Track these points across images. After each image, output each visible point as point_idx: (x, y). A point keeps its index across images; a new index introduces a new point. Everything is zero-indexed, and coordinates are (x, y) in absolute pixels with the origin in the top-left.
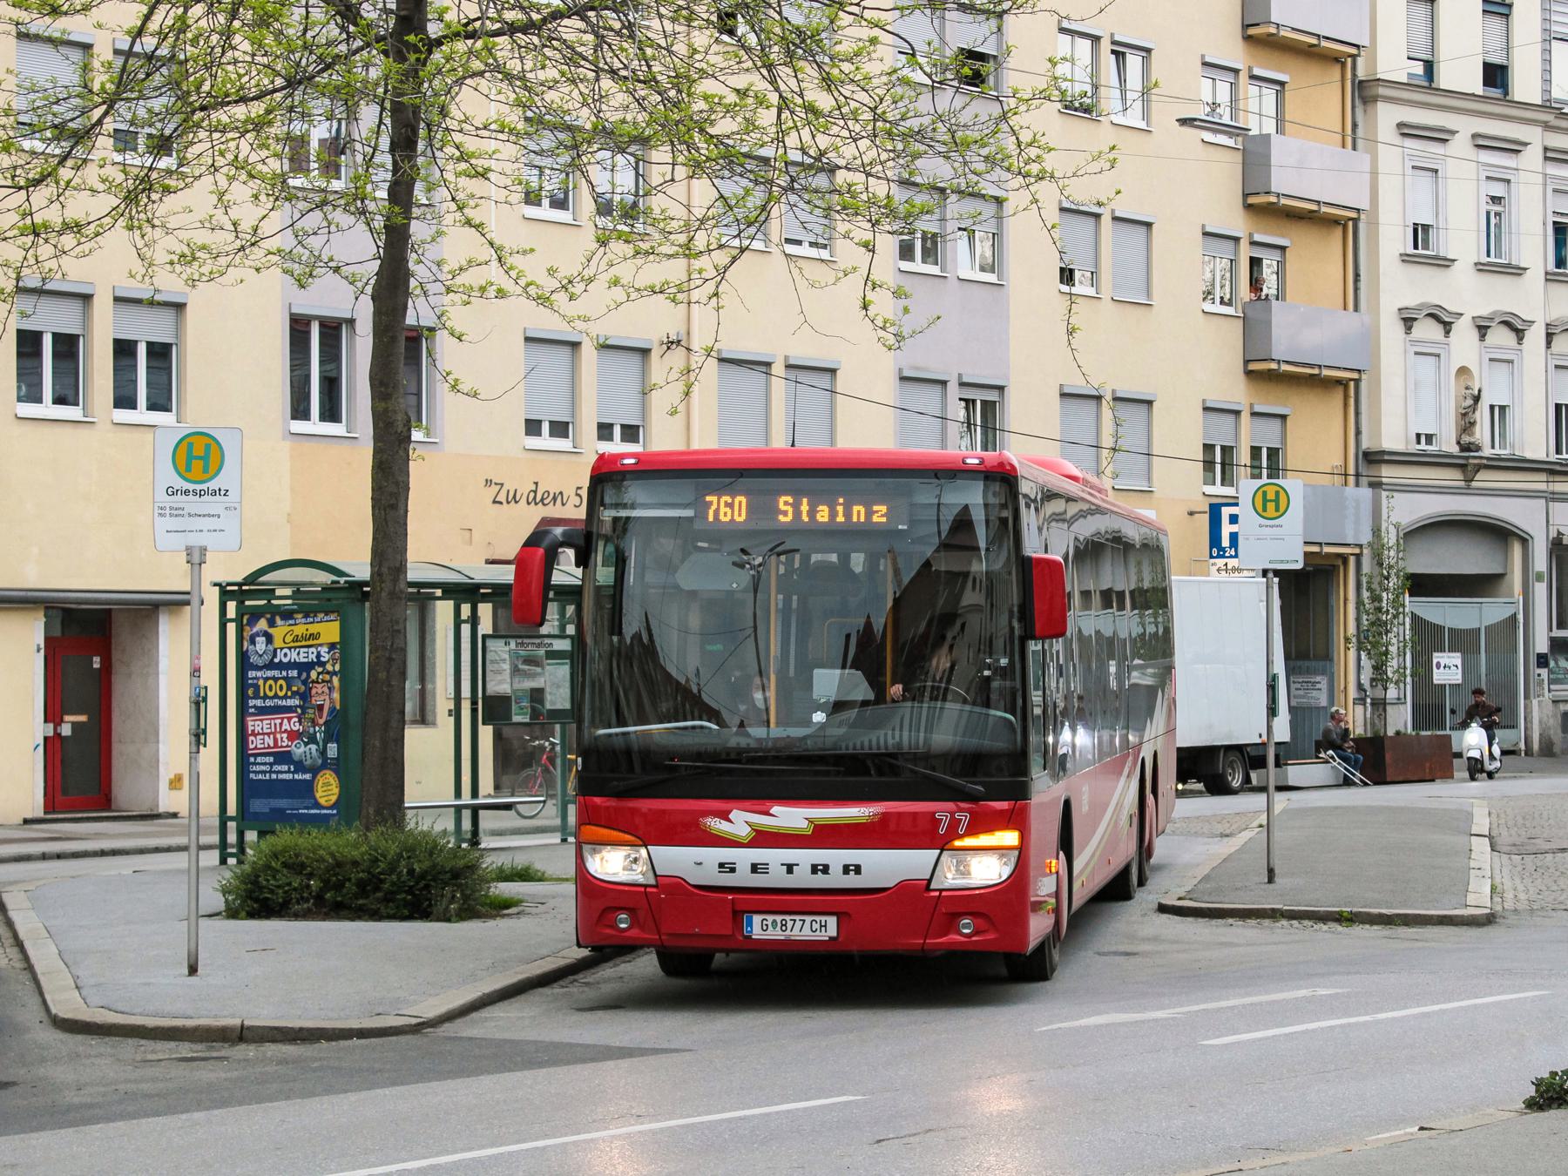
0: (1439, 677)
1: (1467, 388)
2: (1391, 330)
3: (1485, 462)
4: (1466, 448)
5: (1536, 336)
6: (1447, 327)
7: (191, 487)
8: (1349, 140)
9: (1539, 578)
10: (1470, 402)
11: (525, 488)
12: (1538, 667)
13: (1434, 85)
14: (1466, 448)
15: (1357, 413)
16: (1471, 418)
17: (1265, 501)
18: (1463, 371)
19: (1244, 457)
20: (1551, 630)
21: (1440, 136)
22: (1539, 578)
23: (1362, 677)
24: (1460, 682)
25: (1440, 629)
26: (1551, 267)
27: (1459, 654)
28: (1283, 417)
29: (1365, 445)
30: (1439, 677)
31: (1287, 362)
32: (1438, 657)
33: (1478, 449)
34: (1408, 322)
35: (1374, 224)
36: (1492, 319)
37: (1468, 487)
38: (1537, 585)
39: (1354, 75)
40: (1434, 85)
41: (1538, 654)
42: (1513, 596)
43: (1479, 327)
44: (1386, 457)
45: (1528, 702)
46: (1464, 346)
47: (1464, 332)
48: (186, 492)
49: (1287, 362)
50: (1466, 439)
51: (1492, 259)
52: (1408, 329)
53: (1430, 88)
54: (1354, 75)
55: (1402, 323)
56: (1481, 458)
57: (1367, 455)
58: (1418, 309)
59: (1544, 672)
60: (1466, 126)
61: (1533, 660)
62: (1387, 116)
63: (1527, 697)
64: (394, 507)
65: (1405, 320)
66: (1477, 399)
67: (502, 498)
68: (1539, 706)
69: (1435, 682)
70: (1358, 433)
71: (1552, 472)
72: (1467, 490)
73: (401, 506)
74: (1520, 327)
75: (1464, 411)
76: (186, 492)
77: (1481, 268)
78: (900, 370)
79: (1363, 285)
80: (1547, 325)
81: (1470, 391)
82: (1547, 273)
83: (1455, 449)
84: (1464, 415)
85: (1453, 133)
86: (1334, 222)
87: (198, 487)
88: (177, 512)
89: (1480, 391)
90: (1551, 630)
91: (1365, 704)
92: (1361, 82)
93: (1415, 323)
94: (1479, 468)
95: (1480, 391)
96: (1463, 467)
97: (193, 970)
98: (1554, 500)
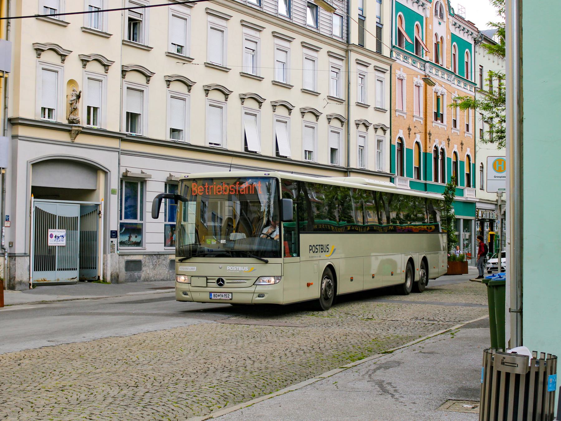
0: (51, 242)
1: (74, 91)
3: (81, 129)
4: (71, 122)
5: (115, 70)
6: (63, 57)
9: (113, 192)
10: (75, 98)
12: (111, 237)
14: (71, 122)
16: (74, 106)
20: (121, 219)
22: (113, 192)
23: (3, 241)
24: (65, 245)
25: (55, 216)
26: (126, 38)
27: (65, 230)
29: (10, 115)
30: (51, 242)
32: (50, 231)
33: (78, 122)
34: (39, 51)
38: (112, 196)
41: (111, 231)
42: (98, 200)
44: (20, 121)
45: (105, 255)
47: (73, 62)
50: (72, 117)
52: (39, 55)
55: (35, 52)
56: (79, 127)
57: (10, 120)
59: (115, 240)
61: (109, 234)
63: (105, 252)
66: (79, 97)
68: (111, 257)
69: (49, 244)
71: (123, 140)
72: (72, 144)
74: (106, 64)
75: (71, 102)
80: (123, 66)
81: (75, 92)
82: (123, 41)
83: (66, 122)
84: (71, 104)
89: (80, 92)
90: (121, 219)
91: (4, 256)
95: (80, 92)
96: (69, 131)
98: (122, 154)
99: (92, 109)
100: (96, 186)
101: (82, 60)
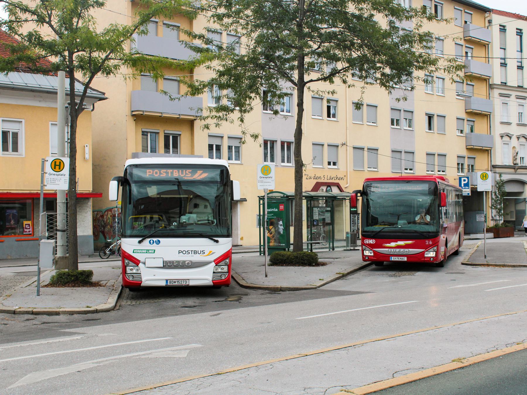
2: (498, 139)
6: (510, 137)
7: (265, 176)
8: (488, 97)
10: (516, 154)
11: (313, 176)
13: (507, 85)
14: (515, 164)
15: (491, 157)
17: (483, 176)
18: (514, 147)
19: (466, 166)
21: (508, 96)
28: (474, 158)
29: (493, 164)
31: (475, 146)
33: (518, 164)
34: (502, 137)
35: (494, 115)
36: (520, 136)
37: (516, 173)
39: (489, 83)
40: (507, 85)
43: (517, 138)
46: (514, 142)
47: (514, 139)
48: (264, 177)
49: (475, 146)
50: (515, 162)
51: (520, 123)
53: (506, 85)
54: (489, 83)
58: (504, 134)
60: (514, 94)
62: (496, 92)
64: (300, 180)
65: (501, 136)
66: (517, 153)
67: (308, 178)
70: (491, 161)
72: (515, 173)
73: (301, 180)
76: (264, 177)
77: (518, 125)
78: (392, 149)
79: (492, 129)
83: (512, 165)
85: (511, 95)
86: (486, 115)
87: (266, 176)
88: (262, 182)
92: (490, 85)
93: (503, 137)
94: (518, 168)
96: (514, 168)
97: (266, 276)
99: (522, 158)
100: (524, 190)
101: (517, 138)
